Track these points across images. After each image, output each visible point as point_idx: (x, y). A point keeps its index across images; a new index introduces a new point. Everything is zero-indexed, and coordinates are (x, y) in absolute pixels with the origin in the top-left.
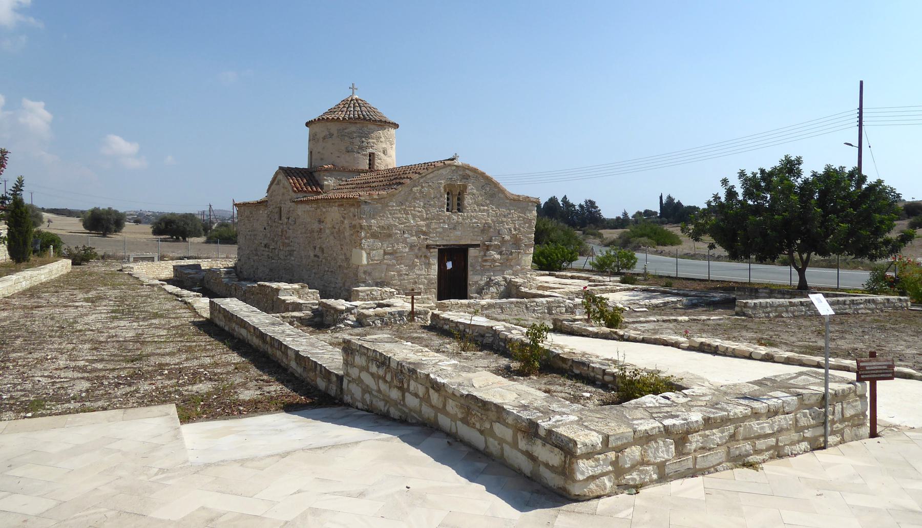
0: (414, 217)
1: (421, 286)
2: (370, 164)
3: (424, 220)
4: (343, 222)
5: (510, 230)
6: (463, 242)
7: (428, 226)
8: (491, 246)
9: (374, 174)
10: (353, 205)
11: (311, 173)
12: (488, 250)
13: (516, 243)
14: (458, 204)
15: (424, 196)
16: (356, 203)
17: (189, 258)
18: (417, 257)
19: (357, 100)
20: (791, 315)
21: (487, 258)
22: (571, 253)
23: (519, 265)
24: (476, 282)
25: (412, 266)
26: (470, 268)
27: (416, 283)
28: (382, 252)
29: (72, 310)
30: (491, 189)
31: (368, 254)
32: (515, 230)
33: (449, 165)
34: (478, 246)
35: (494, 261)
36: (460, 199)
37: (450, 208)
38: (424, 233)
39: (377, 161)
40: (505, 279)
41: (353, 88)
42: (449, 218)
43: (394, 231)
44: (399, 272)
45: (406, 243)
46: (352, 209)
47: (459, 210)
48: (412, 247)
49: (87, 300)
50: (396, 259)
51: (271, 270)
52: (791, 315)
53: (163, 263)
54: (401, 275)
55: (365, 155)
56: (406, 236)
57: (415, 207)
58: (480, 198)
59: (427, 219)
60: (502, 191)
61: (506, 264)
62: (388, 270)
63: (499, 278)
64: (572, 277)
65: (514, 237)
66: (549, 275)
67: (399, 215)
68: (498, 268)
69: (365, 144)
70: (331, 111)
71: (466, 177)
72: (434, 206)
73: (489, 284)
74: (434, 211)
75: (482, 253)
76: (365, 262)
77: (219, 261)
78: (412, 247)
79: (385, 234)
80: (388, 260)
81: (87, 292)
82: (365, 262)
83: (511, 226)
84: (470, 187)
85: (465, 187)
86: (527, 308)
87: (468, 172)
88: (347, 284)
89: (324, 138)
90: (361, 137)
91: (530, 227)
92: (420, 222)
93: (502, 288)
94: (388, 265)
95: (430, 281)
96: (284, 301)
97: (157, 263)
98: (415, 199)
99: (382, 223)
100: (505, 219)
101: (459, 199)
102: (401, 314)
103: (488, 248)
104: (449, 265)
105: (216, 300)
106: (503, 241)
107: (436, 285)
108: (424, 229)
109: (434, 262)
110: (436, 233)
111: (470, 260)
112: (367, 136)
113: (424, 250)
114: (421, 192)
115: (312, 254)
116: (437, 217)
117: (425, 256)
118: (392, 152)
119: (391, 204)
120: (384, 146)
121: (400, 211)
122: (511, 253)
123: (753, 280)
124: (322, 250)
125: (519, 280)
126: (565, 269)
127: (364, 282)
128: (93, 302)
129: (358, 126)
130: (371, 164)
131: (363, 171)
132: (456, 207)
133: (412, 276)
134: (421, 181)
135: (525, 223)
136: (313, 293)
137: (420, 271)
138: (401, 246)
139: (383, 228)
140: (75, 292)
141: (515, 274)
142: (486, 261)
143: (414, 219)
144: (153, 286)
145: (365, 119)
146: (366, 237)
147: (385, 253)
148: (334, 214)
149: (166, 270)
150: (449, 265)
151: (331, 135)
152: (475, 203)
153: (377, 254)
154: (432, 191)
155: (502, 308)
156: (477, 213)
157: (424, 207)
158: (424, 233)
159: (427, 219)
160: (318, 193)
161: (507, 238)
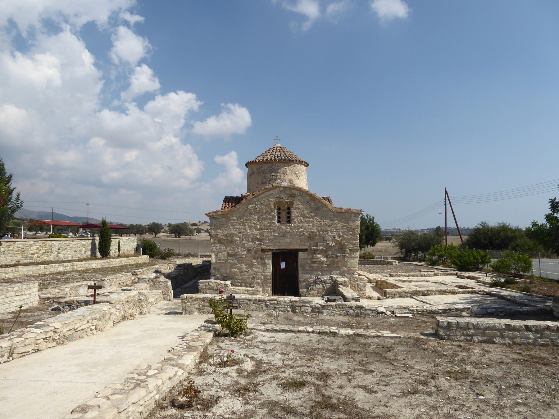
0: (250, 228)
1: (259, 281)
3: (258, 230)
5: (334, 237)
6: (292, 247)
13: (342, 248)
15: (258, 212)
18: (255, 258)
20: (508, 341)
21: (315, 260)
23: (346, 266)
24: (306, 280)
25: (251, 266)
26: (300, 268)
28: (226, 254)
31: (216, 255)
32: (339, 237)
38: (259, 240)
40: (332, 278)
43: (235, 238)
44: (240, 269)
45: (245, 248)
47: (289, 222)
48: (249, 251)
50: (238, 259)
52: (508, 341)
54: (242, 272)
56: (244, 242)
57: (251, 220)
58: (306, 212)
59: (260, 229)
61: (332, 266)
62: (232, 267)
63: (326, 278)
64: (469, 278)
67: (239, 226)
68: (326, 269)
72: (266, 219)
73: (315, 282)
74: (266, 223)
78: (249, 251)
80: (231, 260)
83: (335, 234)
84: (296, 203)
85: (292, 203)
87: (294, 191)
93: (328, 286)
94: (231, 264)
95: (266, 277)
98: (251, 214)
99: (226, 232)
103: (315, 252)
104: (283, 265)
106: (328, 247)
107: (271, 281)
108: (258, 237)
110: (269, 239)
111: (300, 262)
113: (260, 253)
114: (255, 209)
116: (269, 227)
120: (290, 177)
122: (337, 257)
125: (340, 279)
127: (214, 276)
133: (251, 272)
134: (255, 200)
135: (349, 231)
137: (257, 269)
138: (240, 250)
139: (226, 236)
141: (342, 274)
142: (314, 262)
147: (229, 255)
150: (283, 265)
152: (301, 216)
153: (223, 256)
154: (264, 207)
156: (303, 224)
157: (258, 220)
158: (259, 240)
161: (332, 244)
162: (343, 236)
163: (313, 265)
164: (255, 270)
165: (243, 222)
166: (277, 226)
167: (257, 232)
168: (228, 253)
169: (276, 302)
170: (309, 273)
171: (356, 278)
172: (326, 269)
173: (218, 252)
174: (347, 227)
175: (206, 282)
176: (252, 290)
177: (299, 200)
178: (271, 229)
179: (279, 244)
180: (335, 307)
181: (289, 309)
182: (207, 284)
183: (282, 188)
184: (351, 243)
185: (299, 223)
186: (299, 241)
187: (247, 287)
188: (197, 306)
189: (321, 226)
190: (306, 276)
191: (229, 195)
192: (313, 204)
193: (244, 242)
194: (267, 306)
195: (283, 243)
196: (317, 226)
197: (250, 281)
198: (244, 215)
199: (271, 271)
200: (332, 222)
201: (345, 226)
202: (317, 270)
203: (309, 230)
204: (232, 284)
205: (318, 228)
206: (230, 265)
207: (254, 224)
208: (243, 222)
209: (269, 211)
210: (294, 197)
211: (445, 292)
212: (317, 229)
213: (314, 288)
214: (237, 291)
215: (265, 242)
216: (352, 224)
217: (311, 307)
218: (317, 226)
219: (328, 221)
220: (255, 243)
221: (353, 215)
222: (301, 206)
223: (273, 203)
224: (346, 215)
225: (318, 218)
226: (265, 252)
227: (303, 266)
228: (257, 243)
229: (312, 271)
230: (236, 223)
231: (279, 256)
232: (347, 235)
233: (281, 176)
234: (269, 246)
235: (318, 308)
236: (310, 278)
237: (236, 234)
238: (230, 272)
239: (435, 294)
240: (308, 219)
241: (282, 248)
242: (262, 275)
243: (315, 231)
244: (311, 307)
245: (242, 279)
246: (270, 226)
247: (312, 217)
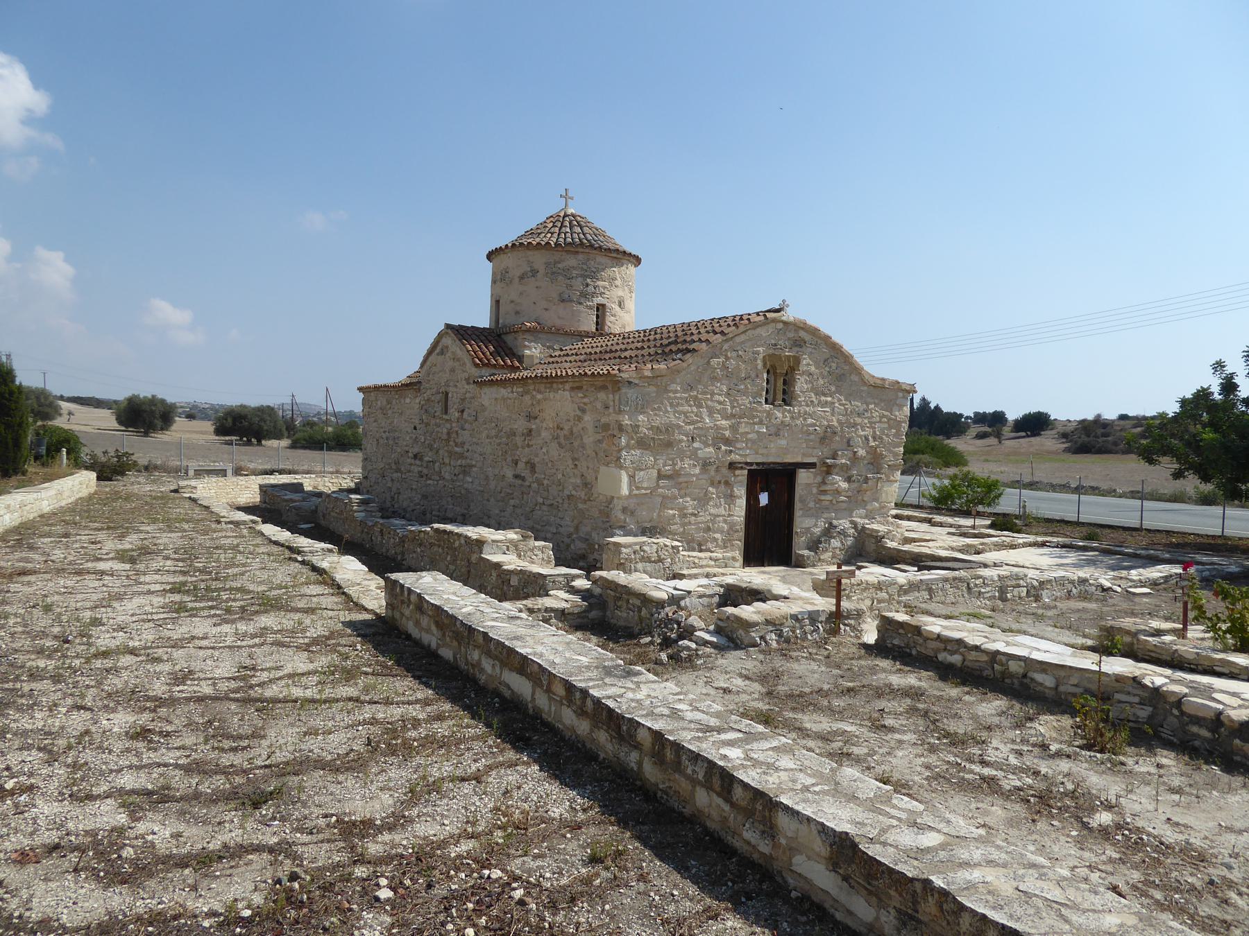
0: (711, 412)
1: (718, 536)
2: (597, 323)
3: (727, 418)
4: (580, 419)
5: (867, 439)
6: (789, 459)
7: (734, 428)
8: (834, 466)
9: (601, 341)
10: (604, 388)
11: (499, 336)
12: (828, 473)
13: (875, 461)
14: (784, 392)
16: (611, 383)
17: (281, 472)
18: (712, 484)
19: (574, 216)
23: (876, 500)
25: (703, 501)
26: (797, 505)
28: (655, 473)
29: (91, 582)
30: (840, 365)
31: (632, 477)
32: (874, 439)
33: (774, 321)
34: (812, 465)
35: (838, 492)
36: (788, 382)
37: (770, 400)
38: (727, 442)
39: (609, 319)
41: (566, 196)
42: (769, 414)
43: (678, 437)
44: (682, 509)
45: (697, 459)
46: (602, 395)
48: (705, 465)
49: (122, 556)
50: (678, 486)
51: (425, 497)
53: (242, 480)
54: (685, 516)
55: (590, 308)
56: (696, 445)
57: (713, 394)
58: (821, 382)
59: (733, 416)
60: (857, 370)
61: (856, 500)
62: (664, 506)
63: (844, 524)
67: (687, 408)
68: (844, 505)
69: (590, 289)
70: (531, 233)
71: (798, 343)
72: (745, 393)
73: (829, 531)
75: (819, 479)
76: (625, 491)
77: (328, 477)
78: (705, 465)
79: (660, 442)
80: (666, 489)
81: (121, 537)
82: (625, 491)
83: (868, 432)
85: (797, 360)
86: (969, 588)
87: (802, 334)
88: (584, 529)
89: (522, 278)
90: (585, 277)
91: (897, 435)
92: (721, 420)
93: (850, 541)
94: (664, 497)
95: (732, 526)
96: (498, 566)
97: (231, 479)
98: (714, 379)
99: (657, 422)
100: (859, 420)
101: (785, 382)
102: (813, 617)
103: (829, 470)
104: (764, 499)
105: (394, 576)
107: (742, 534)
108: (727, 433)
109: (741, 492)
112: (594, 275)
113: (725, 471)
115: (509, 474)
116: (749, 414)
117: (727, 483)
118: (630, 304)
119: (673, 387)
120: (620, 293)
121: (687, 401)
122: (866, 480)
123: (1228, 532)
124: (532, 467)
127: (622, 527)
128: (132, 561)
129: (581, 257)
130: (600, 323)
131: (588, 335)
132: (780, 396)
133: (704, 517)
134: (726, 347)
135: (890, 428)
136: (542, 549)
137: (717, 509)
138: (687, 463)
140: (101, 536)
141: (870, 516)
142: (825, 492)
144: (237, 524)
145: (592, 246)
146: (628, 447)
147: (660, 476)
148: (561, 404)
149: (249, 490)
150: (764, 499)
151: (534, 272)
152: (813, 389)
153: (647, 478)
155: (930, 590)
156: (816, 407)
158: (727, 442)
159: (733, 416)
160: (514, 369)
161: (861, 452)
164: (712, 511)
165: (696, 398)
168: (659, 471)
170: (812, 516)
172: (844, 505)
173: (635, 469)
175: (636, 544)
178: (754, 417)
179: (764, 451)
183: (780, 326)
184: (891, 452)
187: (694, 550)
191: (455, 322)
192: (834, 365)
195: (773, 451)
197: (699, 536)
198: (699, 382)
199: (743, 513)
201: (884, 416)
206: (660, 500)
207: (720, 403)
208: (696, 398)
209: (753, 375)
212: (838, 421)
215: (738, 446)
220: (719, 448)
221: (900, 394)
222: (813, 368)
223: (761, 356)
224: (890, 392)
226: (737, 468)
230: (681, 398)
232: (887, 436)
233: (605, 288)
236: (816, 525)
237: (679, 427)
238: (659, 516)
240: (823, 398)
241: (771, 460)
242: (725, 521)
243: (835, 424)
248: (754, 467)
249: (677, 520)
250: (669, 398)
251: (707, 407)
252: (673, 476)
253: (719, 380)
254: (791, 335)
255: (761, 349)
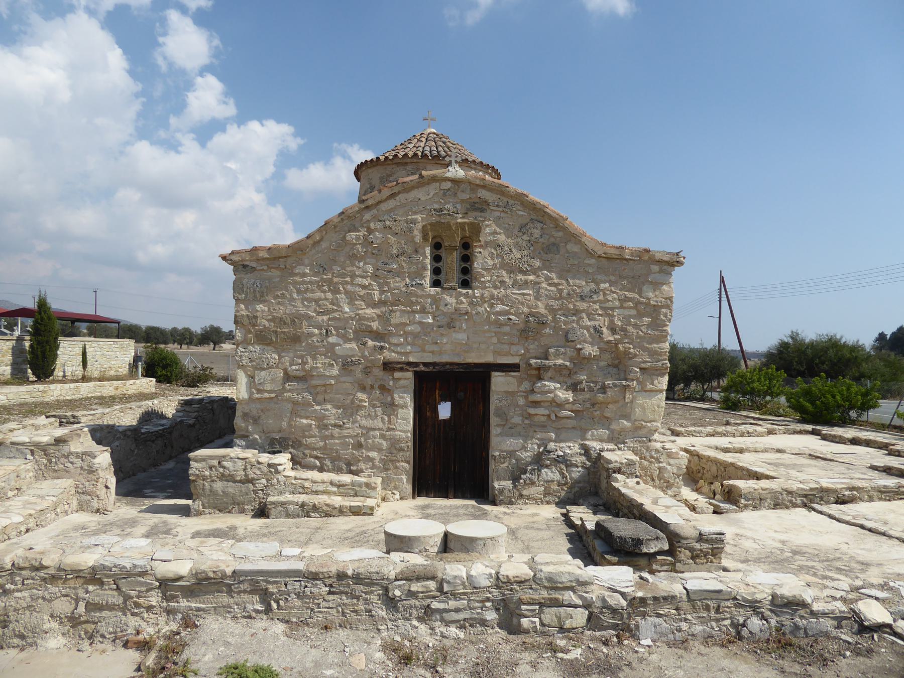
0: (352, 298)
1: (373, 454)
3: (373, 305)
5: (597, 330)
6: (473, 358)
12: (540, 378)
13: (618, 363)
15: (376, 252)
18: (363, 389)
21: (538, 397)
22: (865, 395)
23: (627, 417)
24: (512, 454)
25: (351, 410)
26: (494, 420)
27: (359, 446)
28: (280, 374)
31: (251, 377)
32: (613, 330)
34: (514, 367)
38: (377, 336)
40: (586, 451)
42: (435, 300)
43: (306, 329)
44: (320, 418)
45: (335, 357)
47: (465, 284)
48: (347, 365)
56: (332, 340)
57: (354, 276)
58: (516, 254)
59: (382, 303)
60: (574, 237)
61: (589, 415)
62: (295, 414)
63: (571, 448)
64: (855, 441)
65: (610, 348)
66: (814, 433)
67: (319, 295)
68: (572, 423)
71: (479, 206)
72: (399, 274)
73: (539, 461)
74: (399, 284)
75: (526, 385)
78: (347, 365)
80: (293, 392)
83: (602, 322)
84: (490, 230)
85: (476, 229)
87: (483, 194)
93: (576, 473)
94: (295, 403)
98: (354, 257)
99: (280, 311)
100: (582, 305)
103: (539, 373)
104: (445, 411)
106: (580, 360)
107: (410, 454)
108: (375, 325)
111: (495, 401)
113: (378, 372)
116: (407, 299)
121: (320, 287)
122: (604, 389)
125: (616, 456)
126: (852, 423)
127: (244, 437)
133: (352, 430)
134: (367, 216)
135: (640, 315)
137: (370, 419)
139: (281, 321)
141: (617, 439)
142: (536, 404)
143: (351, 303)
145: (424, 156)
147: (288, 377)
150: (445, 411)
152: (503, 266)
153: (271, 379)
157: (375, 276)
158: (377, 336)
159: (382, 303)
161: (590, 350)
162: (623, 330)
163: (532, 411)
164: (364, 422)
165: (330, 282)
166: (429, 296)
167: (370, 312)
168: (285, 371)
169: (432, 585)
170: (520, 435)
171: (657, 451)
172: (572, 423)
173: (256, 368)
174: (637, 304)
175: (212, 458)
176: (353, 484)
177: (497, 221)
178: (412, 304)
179: (435, 348)
180: (685, 605)
181: (492, 616)
182: (215, 463)
183: (448, 185)
184: (645, 350)
185: (495, 287)
186: (495, 340)
187: (339, 471)
188: (63, 606)
189: (561, 298)
190: (511, 443)
192: (537, 233)
193: (332, 340)
194: (390, 602)
196: (549, 297)
197: (348, 453)
198: (334, 261)
199: (410, 427)
200: (592, 285)
201: (627, 299)
202: (543, 426)
203: (526, 310)
204: (296, 462)
205: (552, 302)
206: (289, 406)
207: (364, 287)
208: (330, 282)
209: (409, 249)
210: (482, 210)
211: (897, 493)
212: (547, 307)
213: (535, 478)
214: (307, 484)
215: (394, 340)
216: (651, 295)
217: (587, 605)
218: (549, 297)
219: (581, 284)
220: (364, 344)
221: (655, 268)
222: (502, 238)
223: (420, 226)
225: (553, 275)
226: (394, 370)
227: (502, 415)
228: (370, 343)
229: (530, 427)
230: (311, 283)
231: (431, 382)
232: (635, 326)
234: (406, 354)
235: (614, 611)
236: (524, 448)
237: (309, 318)
238: (290, 425)
239: (871, 499)
241: (445, 359)
242: (383, 437)
244: (587, 605)
245: (325, 448)
246: (409, 294)
247: (535, 272)
248: (423, 368)
249: (316, 431)
250: (295, 283)
251: (347, 292)
252: (303, 378)
253: (361, 259)
254: (465, 196)
255: (419, 217)
